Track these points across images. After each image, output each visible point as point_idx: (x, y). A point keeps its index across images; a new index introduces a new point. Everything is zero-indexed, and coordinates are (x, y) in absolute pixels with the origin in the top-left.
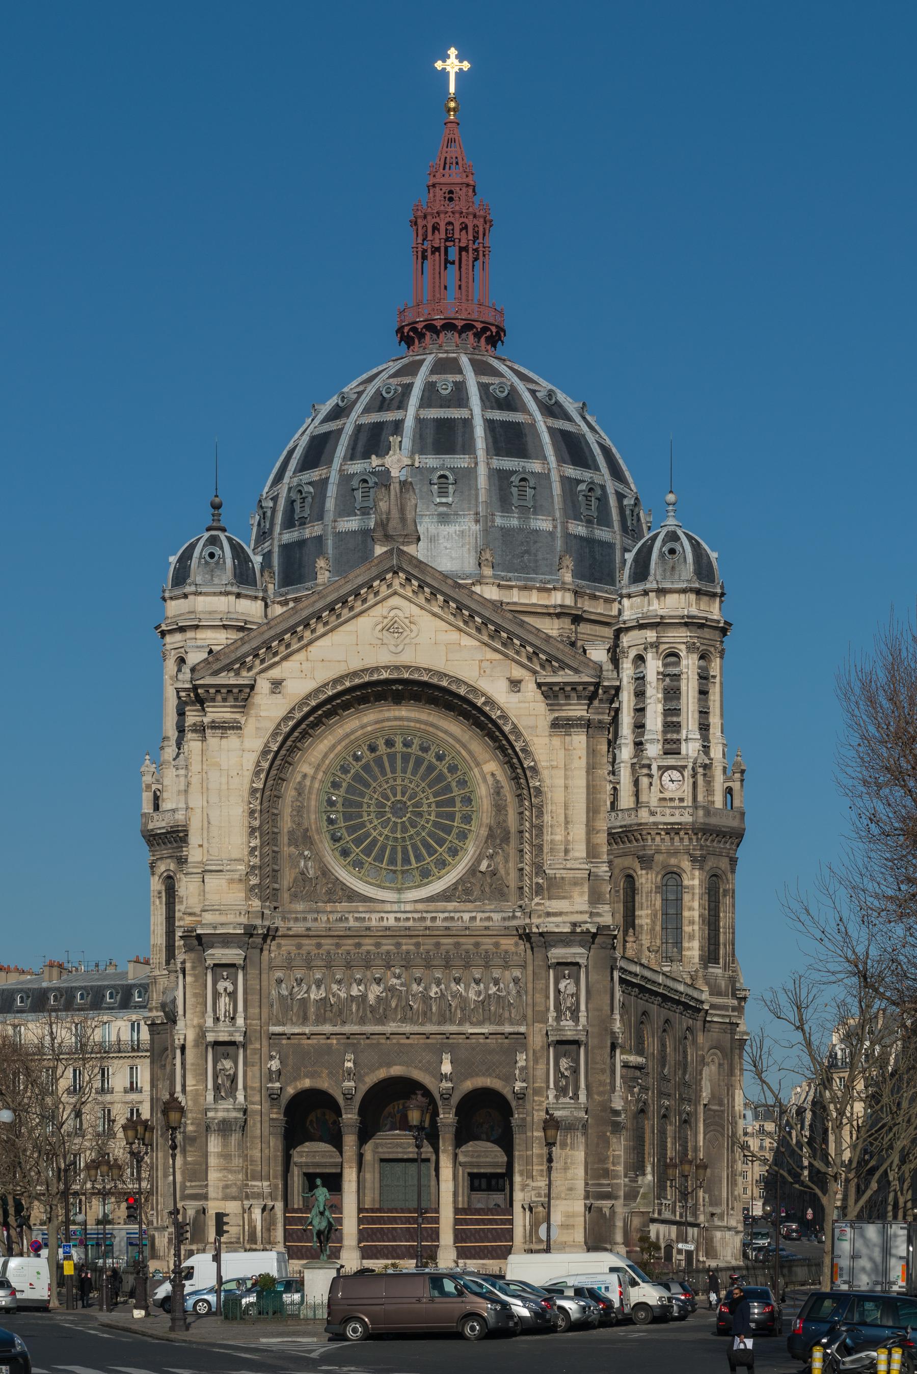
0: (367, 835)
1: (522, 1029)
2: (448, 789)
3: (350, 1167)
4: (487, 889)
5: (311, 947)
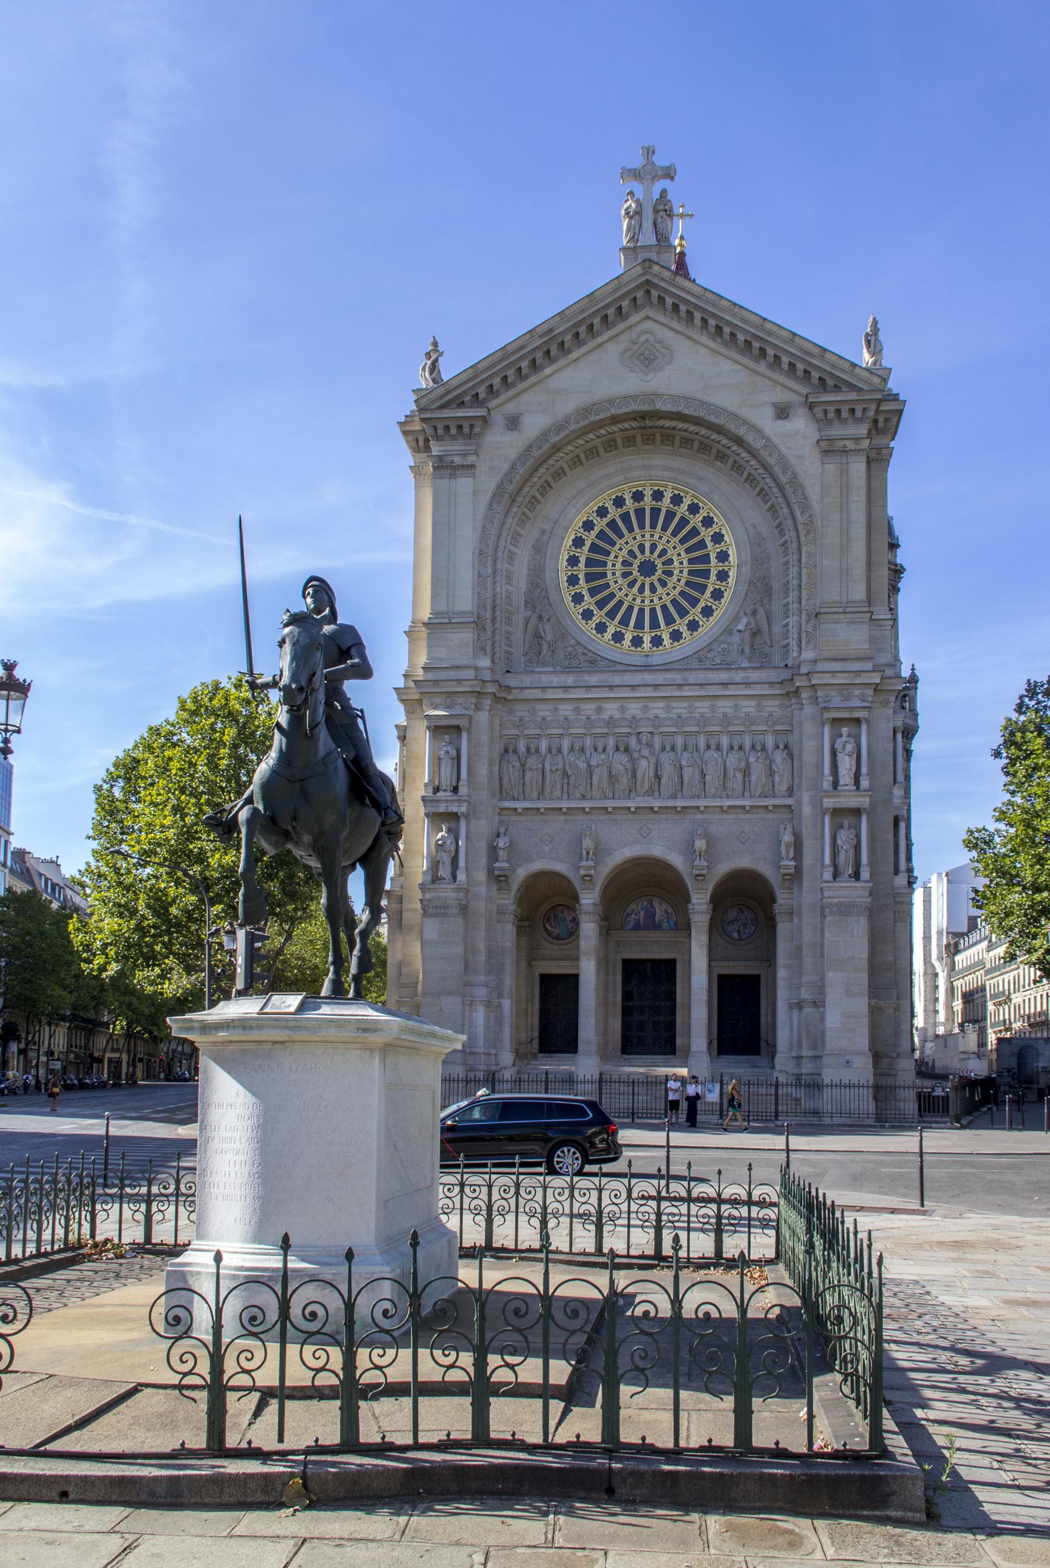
0: (612, 595)
1: (789, 801)
2: (702, 544)
3: (589, 960)
4: (747, 651)
5: (548, 713)
